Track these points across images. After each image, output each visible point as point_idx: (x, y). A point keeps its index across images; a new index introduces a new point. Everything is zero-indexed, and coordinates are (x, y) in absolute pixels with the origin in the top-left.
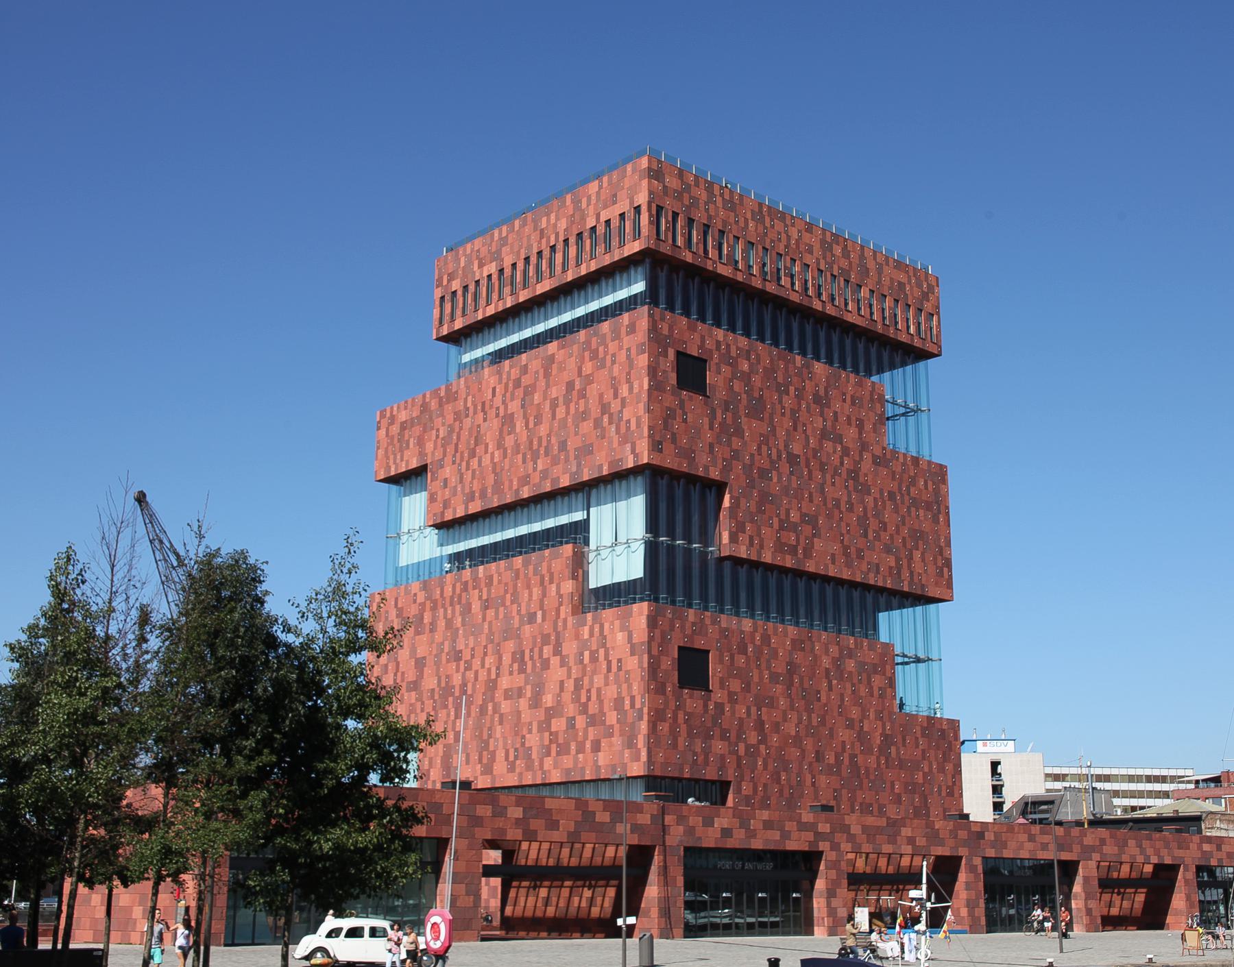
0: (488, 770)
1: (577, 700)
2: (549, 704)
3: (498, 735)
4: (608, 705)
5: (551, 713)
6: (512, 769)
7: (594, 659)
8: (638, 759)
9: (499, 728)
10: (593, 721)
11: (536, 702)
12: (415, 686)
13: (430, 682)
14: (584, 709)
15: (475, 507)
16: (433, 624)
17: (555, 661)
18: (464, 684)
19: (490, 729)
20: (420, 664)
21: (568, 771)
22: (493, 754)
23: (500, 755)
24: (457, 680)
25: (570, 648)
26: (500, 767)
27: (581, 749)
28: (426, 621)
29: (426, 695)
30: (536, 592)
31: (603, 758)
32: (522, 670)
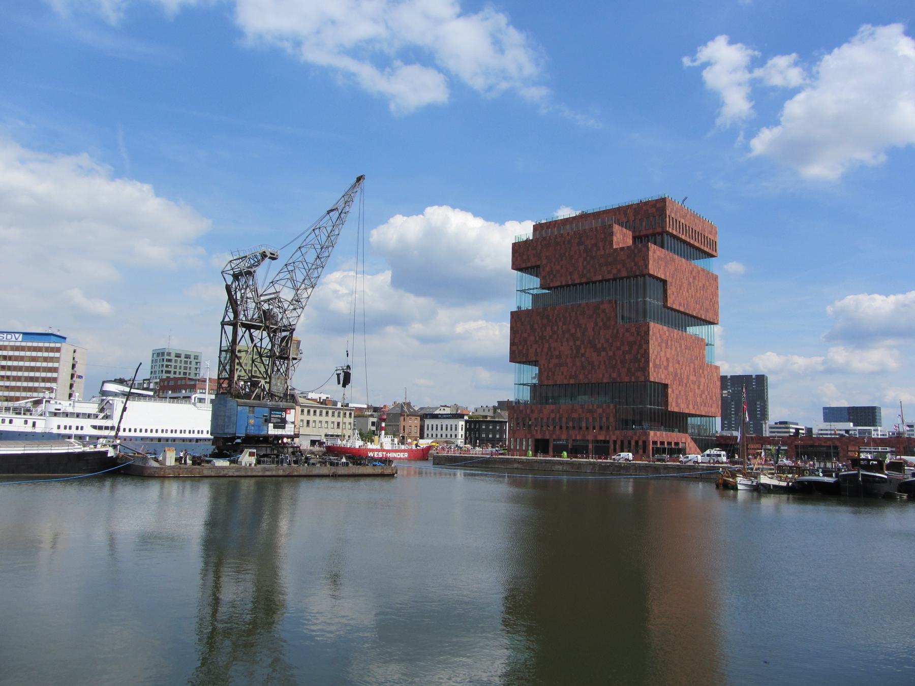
0: (688, 407)
1: (707, 390)
2: (702, 389)
3: (690, 395)
4: (713, 394)
5: (703, 392)
6: (694, 408)
7: (710, 379)
8: (719, 412)
9: (690, 393)
10: (711, 398)
11: (699, 388)
12: (666, 368)
13: (671, 369)
14: (709, 394)
15: (682, 309)
16: (671, 346)
17: (703, 375)
18: (681, 374)
19: (688, 392)
20: (667, 360)
21: (706, 412)
22: (689, 401)
23: (691, 402)
24: (679, 371)
25: (706, 372)
26: (691, 407)
27: (708, 406)
28: (669, 344)
29: (671, 373)
30: (698, 350)
31: (713, 410)
32: (695, 376)
